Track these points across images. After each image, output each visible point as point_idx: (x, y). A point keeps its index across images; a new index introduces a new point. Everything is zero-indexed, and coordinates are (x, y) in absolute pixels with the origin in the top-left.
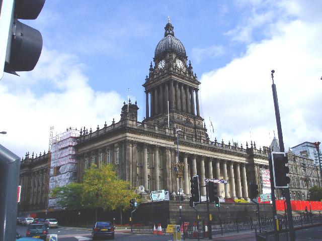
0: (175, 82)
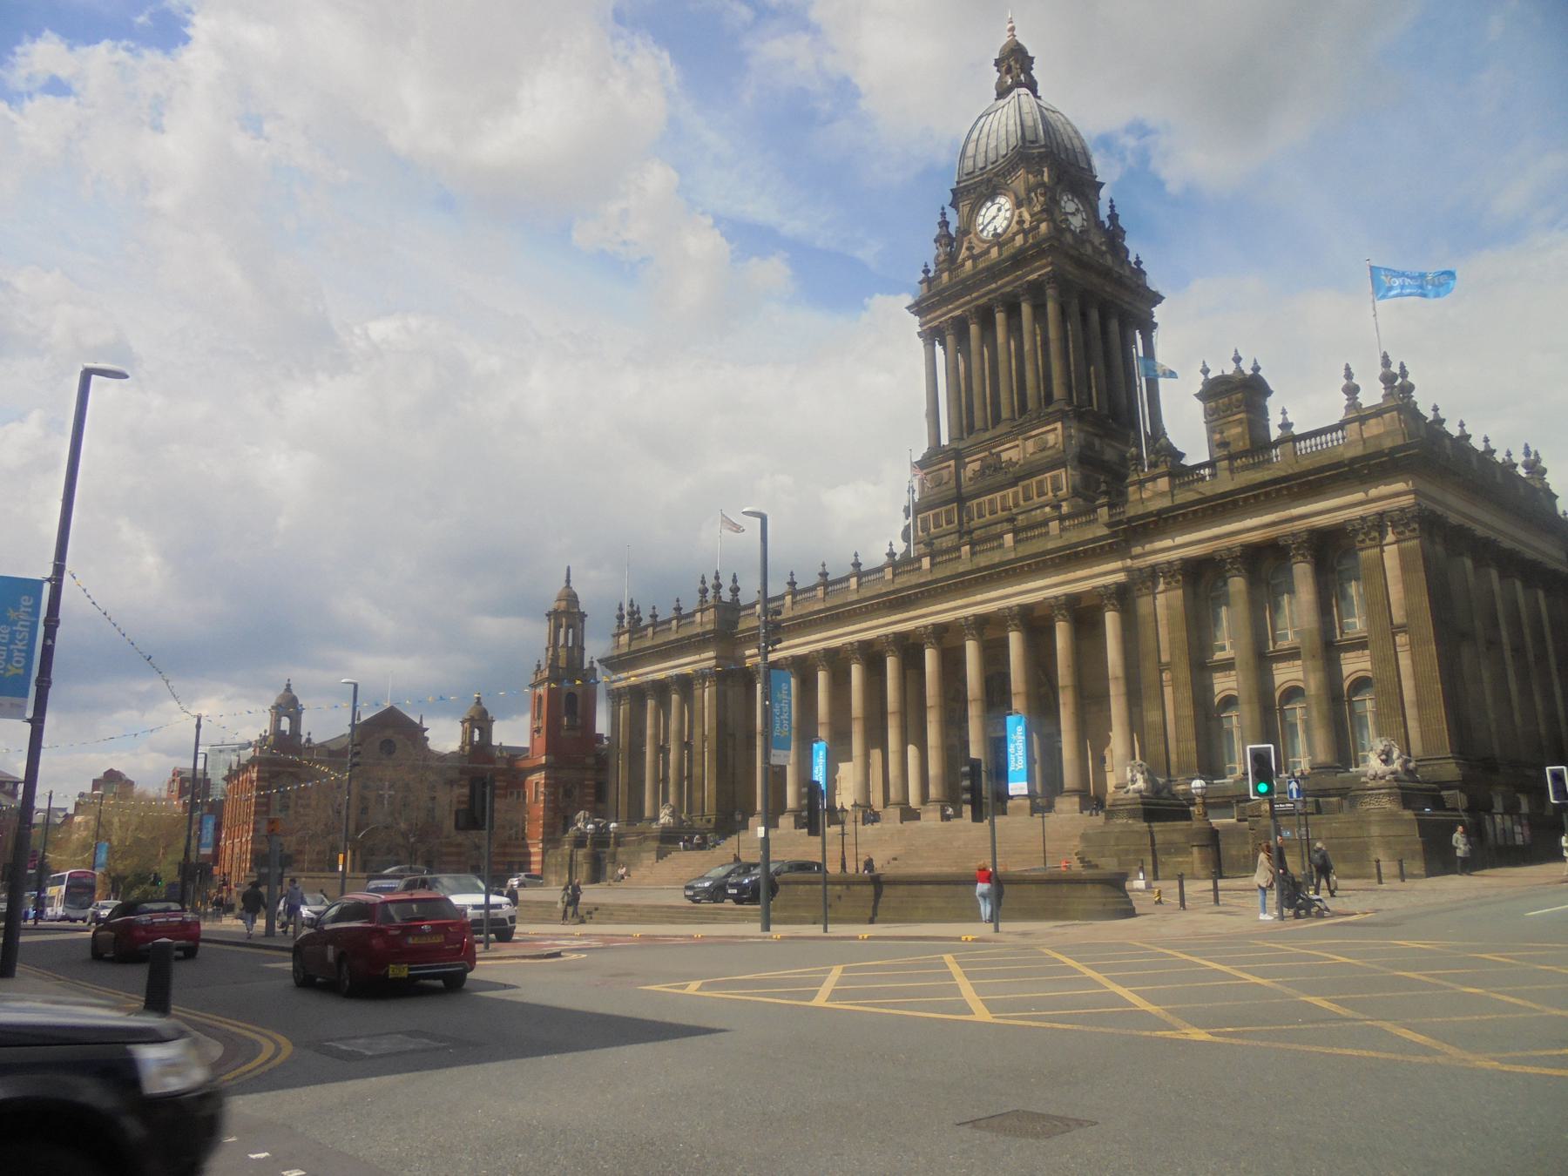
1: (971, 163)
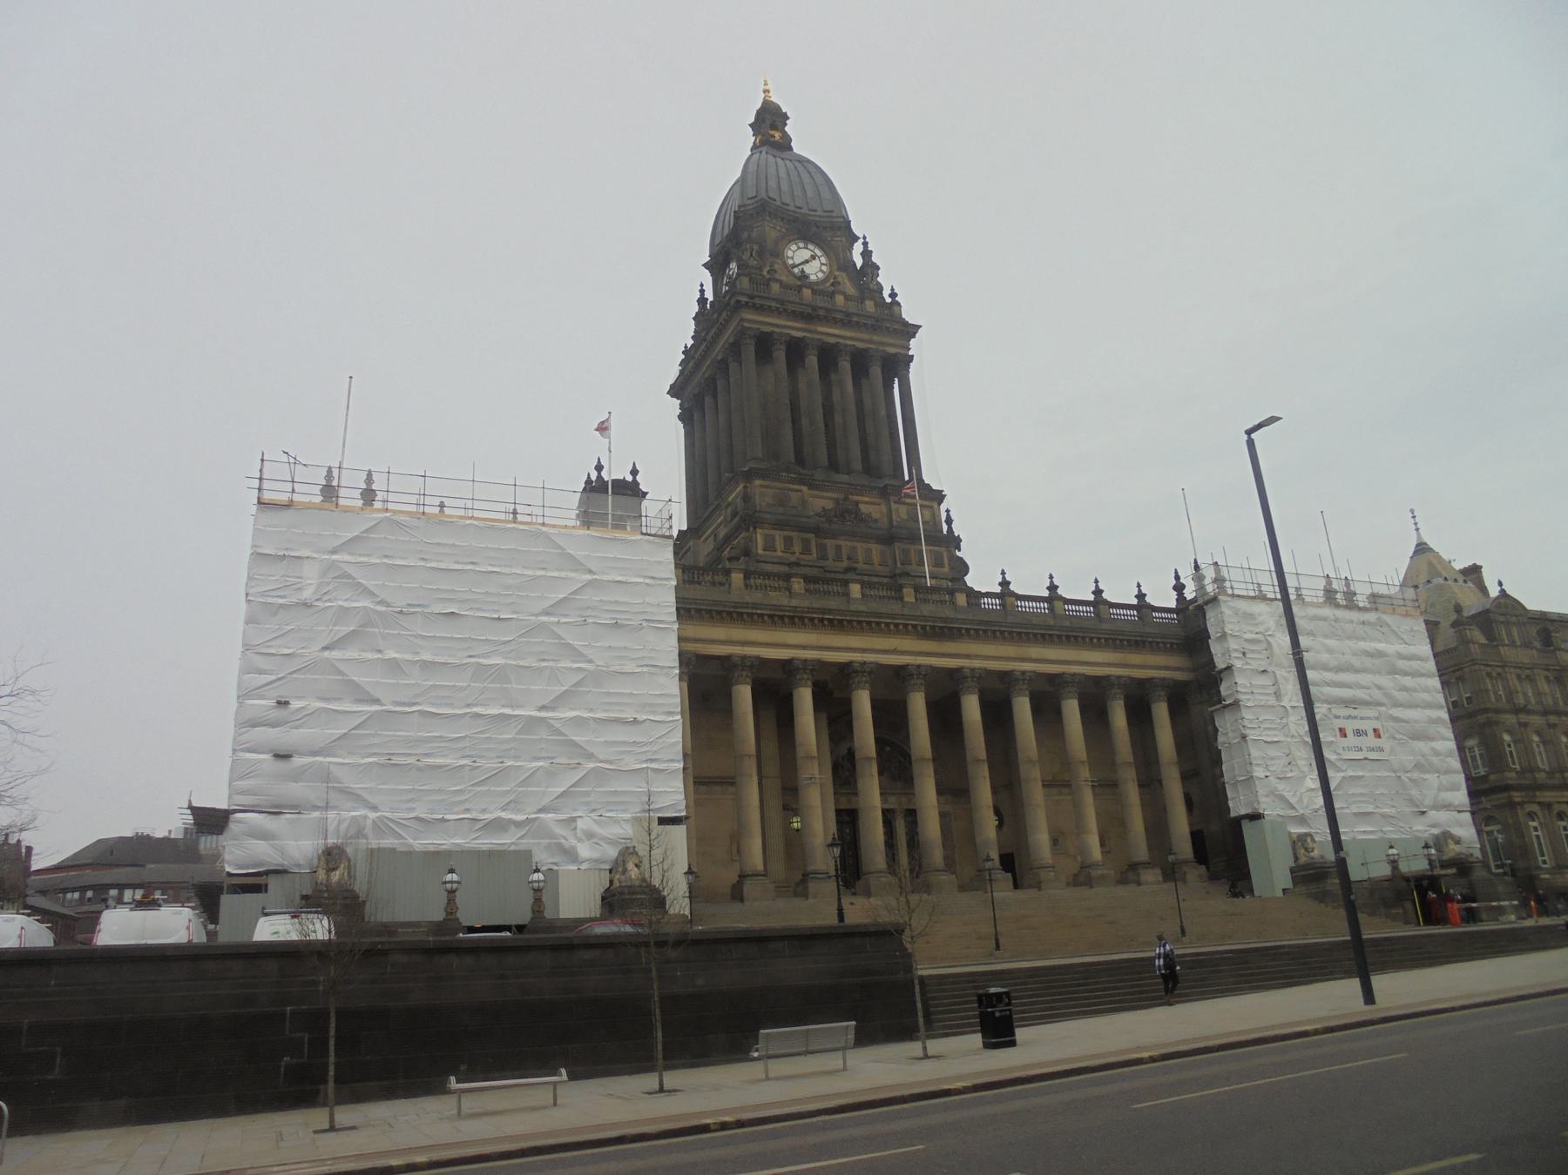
0: (764, 344)
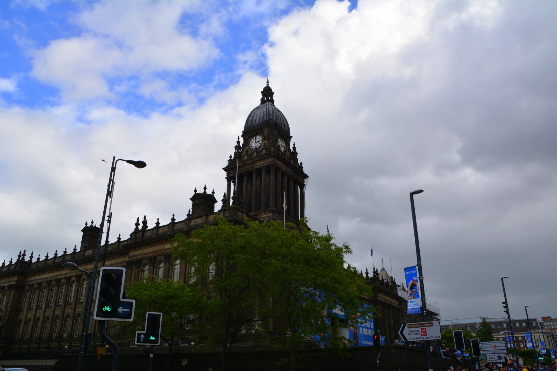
0: (278, 169)
1: (249, 123)
